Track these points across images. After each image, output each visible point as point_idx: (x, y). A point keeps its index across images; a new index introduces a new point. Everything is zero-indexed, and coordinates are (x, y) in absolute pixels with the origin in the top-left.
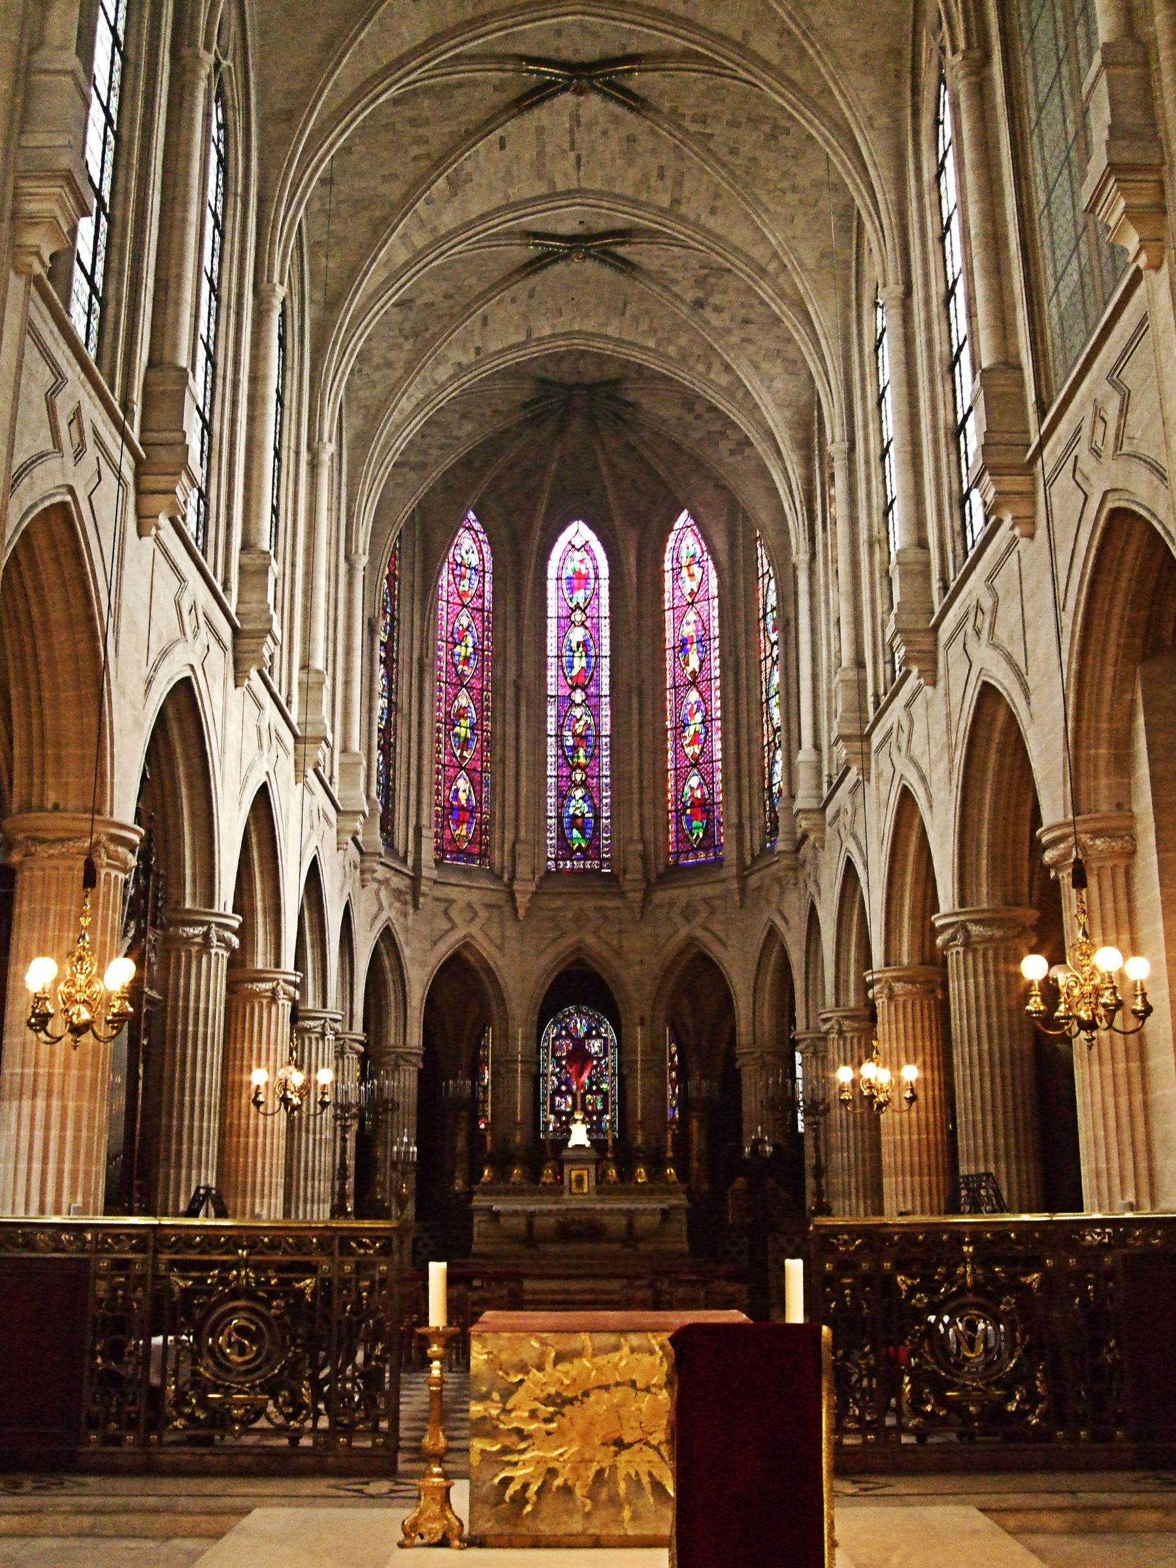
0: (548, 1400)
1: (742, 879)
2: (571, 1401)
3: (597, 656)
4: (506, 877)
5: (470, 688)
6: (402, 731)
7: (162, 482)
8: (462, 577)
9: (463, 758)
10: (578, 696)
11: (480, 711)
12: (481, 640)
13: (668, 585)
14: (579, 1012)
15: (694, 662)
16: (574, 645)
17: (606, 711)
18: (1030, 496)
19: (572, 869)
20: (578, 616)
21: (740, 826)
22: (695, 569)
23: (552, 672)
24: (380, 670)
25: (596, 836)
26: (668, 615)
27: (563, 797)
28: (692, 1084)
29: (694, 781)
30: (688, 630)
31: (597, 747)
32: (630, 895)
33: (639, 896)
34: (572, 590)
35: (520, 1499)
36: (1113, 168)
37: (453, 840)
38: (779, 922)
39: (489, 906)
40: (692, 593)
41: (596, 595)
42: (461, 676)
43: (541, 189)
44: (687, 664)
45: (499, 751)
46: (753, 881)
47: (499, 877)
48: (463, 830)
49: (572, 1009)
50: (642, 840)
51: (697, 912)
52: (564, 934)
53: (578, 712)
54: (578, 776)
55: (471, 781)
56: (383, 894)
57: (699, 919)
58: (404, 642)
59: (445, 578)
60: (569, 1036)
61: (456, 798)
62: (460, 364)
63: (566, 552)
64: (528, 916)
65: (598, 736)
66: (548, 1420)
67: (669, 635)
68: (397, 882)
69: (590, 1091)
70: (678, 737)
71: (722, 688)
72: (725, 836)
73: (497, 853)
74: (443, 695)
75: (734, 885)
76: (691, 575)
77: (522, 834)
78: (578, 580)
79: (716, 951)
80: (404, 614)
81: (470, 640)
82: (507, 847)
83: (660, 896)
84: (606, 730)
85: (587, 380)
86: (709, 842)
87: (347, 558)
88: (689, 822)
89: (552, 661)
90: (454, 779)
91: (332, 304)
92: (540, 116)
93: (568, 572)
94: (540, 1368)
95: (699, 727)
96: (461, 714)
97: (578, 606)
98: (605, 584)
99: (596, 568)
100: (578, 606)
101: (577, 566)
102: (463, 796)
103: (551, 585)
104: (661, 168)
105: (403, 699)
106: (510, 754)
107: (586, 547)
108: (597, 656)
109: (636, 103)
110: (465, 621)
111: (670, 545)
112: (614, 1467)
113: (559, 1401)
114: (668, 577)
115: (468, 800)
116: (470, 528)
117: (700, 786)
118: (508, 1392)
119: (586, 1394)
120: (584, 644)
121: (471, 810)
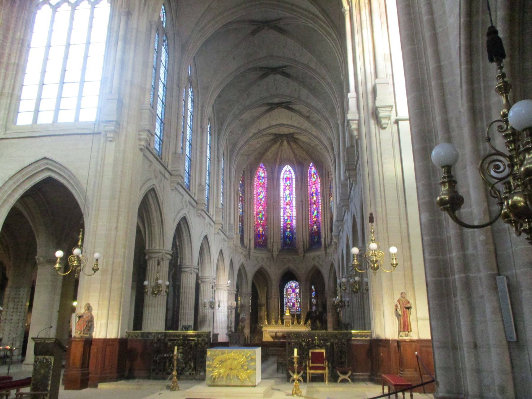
0: (220, 361)
1: (326, 250)
2: (224, 361)
3: (292, 197)
4: (271, 251)
5: (262, 206)
6: (246, 217)
8: (260, 179)
9: (261, 222)
11: (265, 211)
12: (265, 194)
13: (309, 180)
14: (293, 282)
15: (315, 198)
16: (287, 195)
17: (294, 210)
18: (355, 176)
19: (287, 249)
20: (288, 188)
21: (325, 238)
22: (315, 176)
23: (282, 202)
26: (309, 187)
29: (315, 227)
30: (313, 190)
31: (293, 219)
32: (300, 255)
33: (302, 255)
34: (286, 181)
35: (215, 379)
37: (258, 242)
38: (333, 261)
39: (267, 258)
40: (314, 182)
41: (292, 182)
42: (260, 203)
44: (313, 198)
45: (269, 221)
46: (328, 251)
47: (270, 251)
48: (261, 240)
49: (292, 281)
54: (288, 226)
55: (263, 228)
56: (241, 256)
58: (246, 195)
59: (256, 179)
60: (291, 288)
61: (259, 232)
62: (254, 133)
63: (285, 172)
64: (276, 259)
65: (293, 216)
66: (220, 365)
67: (309, 192)
68: (244, 253)
70: (311, 216)
71: (321, 204)
72: (323, 240)
73: (269, 246)
74: (256, 208)
75: (324, 252)
76: (314, 177)
77: (275, 240)
78: (287, 179)
79: (320, 267)
80: (246, 189)
81: (262, 194)
82: (271, 244)
83: (308, 255)
84: (294, 214)
85: (286, 133)
86: (319, 242)
87: (230, 179)
88: (314, 237)
89: (282, 199)
90: (258, 228)
91: (222, 124)
92: (267, 79)
93: (285, 177)
94: (218, 355)
95: (316, 214)
96: (260, 212)
97: (288, 185)
98: (294, 180)
99: (292, 176)
100: (288, 185)
101: (287, 175)
102: (260, 231)
103: (281, 180)
104: (295, 89)
105: (246, 209)
107: (290, 171)
108: (292, 197)
109: (288, 75)
111: (309, 170)
112: (230, 373)
113: (222, 362)
114: (309, 178)
115: (262, 232)
116: (262, 168)
117: (316, 228)
118: (213, 360)
119: (226, 360)
120: (289, 194)
121: (263, 235)
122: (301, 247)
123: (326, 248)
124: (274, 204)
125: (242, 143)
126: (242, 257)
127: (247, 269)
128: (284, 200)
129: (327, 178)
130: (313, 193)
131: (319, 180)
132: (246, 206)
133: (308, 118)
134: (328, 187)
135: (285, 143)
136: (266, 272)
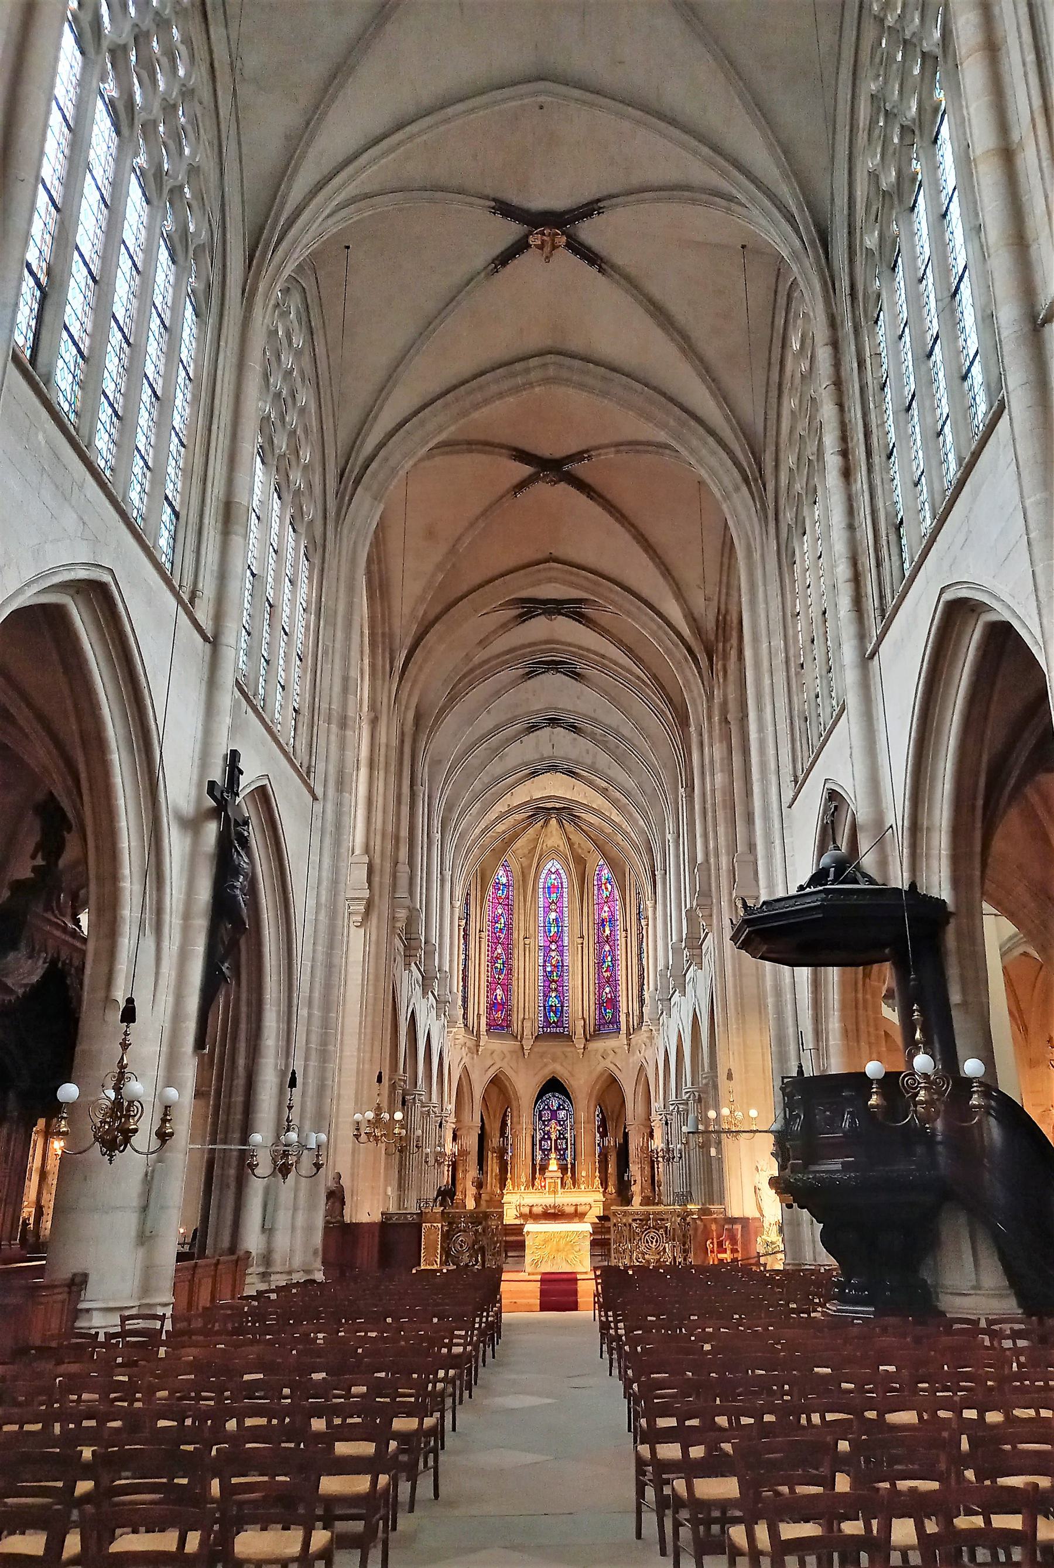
7: (413, 952)
8: (499, 889)
10: (553, 947)
14: (554, 1096)
15: (607, 932)
20: (553, 907)
21: (628, 1014)
22: (609, 887)
24: (462, 941)
25: (562, 1016)
27: (546, 996)
28: (606, 1139)
29: (607, 990)
30: (605, 915)
34: (550, 894)
36: (697, 905)
38: (645, 1064)
39: (510, 1052)
43: (537, 756)
50: (583, 1018)
51: (608, 1055)
52: (546, 1065)
53: (553, 954)
54: (553, 986)
57: (608, 1060)
58: (472, 924)
61: (496, 999)
69: (559, 1138)
72: (623, 1018)
77: (527, 1017)
78: (551, 889)
79: (617, 1072)
83: (593, 1045)
86: (615, 1021)
96: (497, 958)
102: (499, 998)
105: (472, 952)
106: (521, 976)
107: (557, 872)
110: (500, 911)
121: (503, 1004)
122: (580, 1031)
123: (628, 1034)
124: (527, 941)
125: (477, 831)
126: (464, 1051)
127: (473, 1077)
128: (545, 932)
129: (633, 894)
130: (603, 920)
131: (617, 896)
132: (472, 945)
133: (604, 792)
134: (634, 911)
135: (553, 822)
136: (508, 1079)
